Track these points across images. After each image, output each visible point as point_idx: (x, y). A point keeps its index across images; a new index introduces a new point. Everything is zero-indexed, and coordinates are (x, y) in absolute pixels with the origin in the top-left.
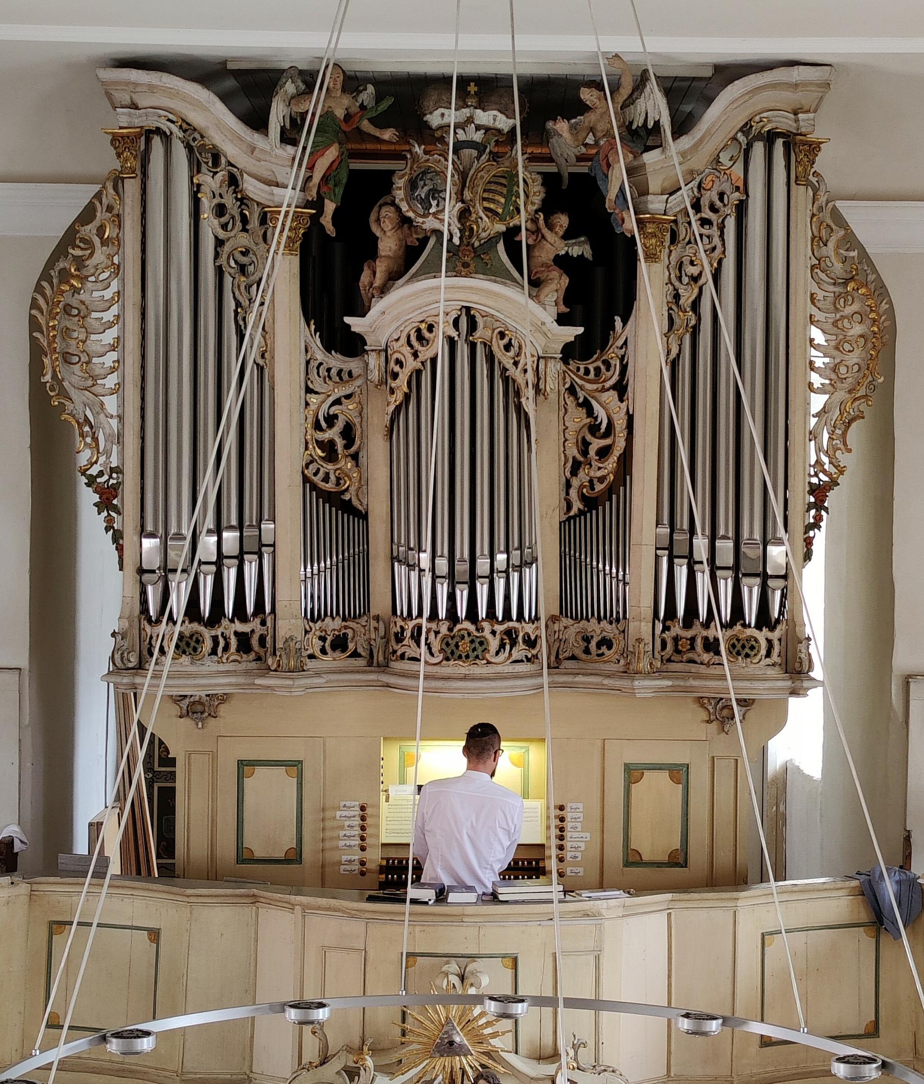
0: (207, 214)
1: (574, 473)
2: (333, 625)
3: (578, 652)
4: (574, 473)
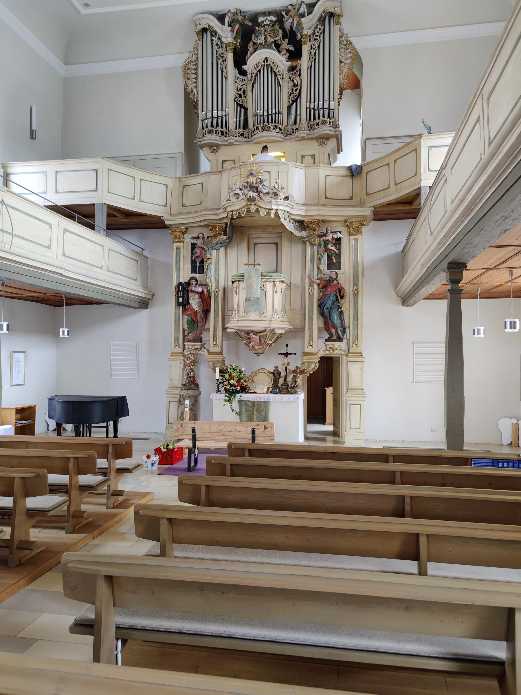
0: (215, 43)
2: (241, 131)
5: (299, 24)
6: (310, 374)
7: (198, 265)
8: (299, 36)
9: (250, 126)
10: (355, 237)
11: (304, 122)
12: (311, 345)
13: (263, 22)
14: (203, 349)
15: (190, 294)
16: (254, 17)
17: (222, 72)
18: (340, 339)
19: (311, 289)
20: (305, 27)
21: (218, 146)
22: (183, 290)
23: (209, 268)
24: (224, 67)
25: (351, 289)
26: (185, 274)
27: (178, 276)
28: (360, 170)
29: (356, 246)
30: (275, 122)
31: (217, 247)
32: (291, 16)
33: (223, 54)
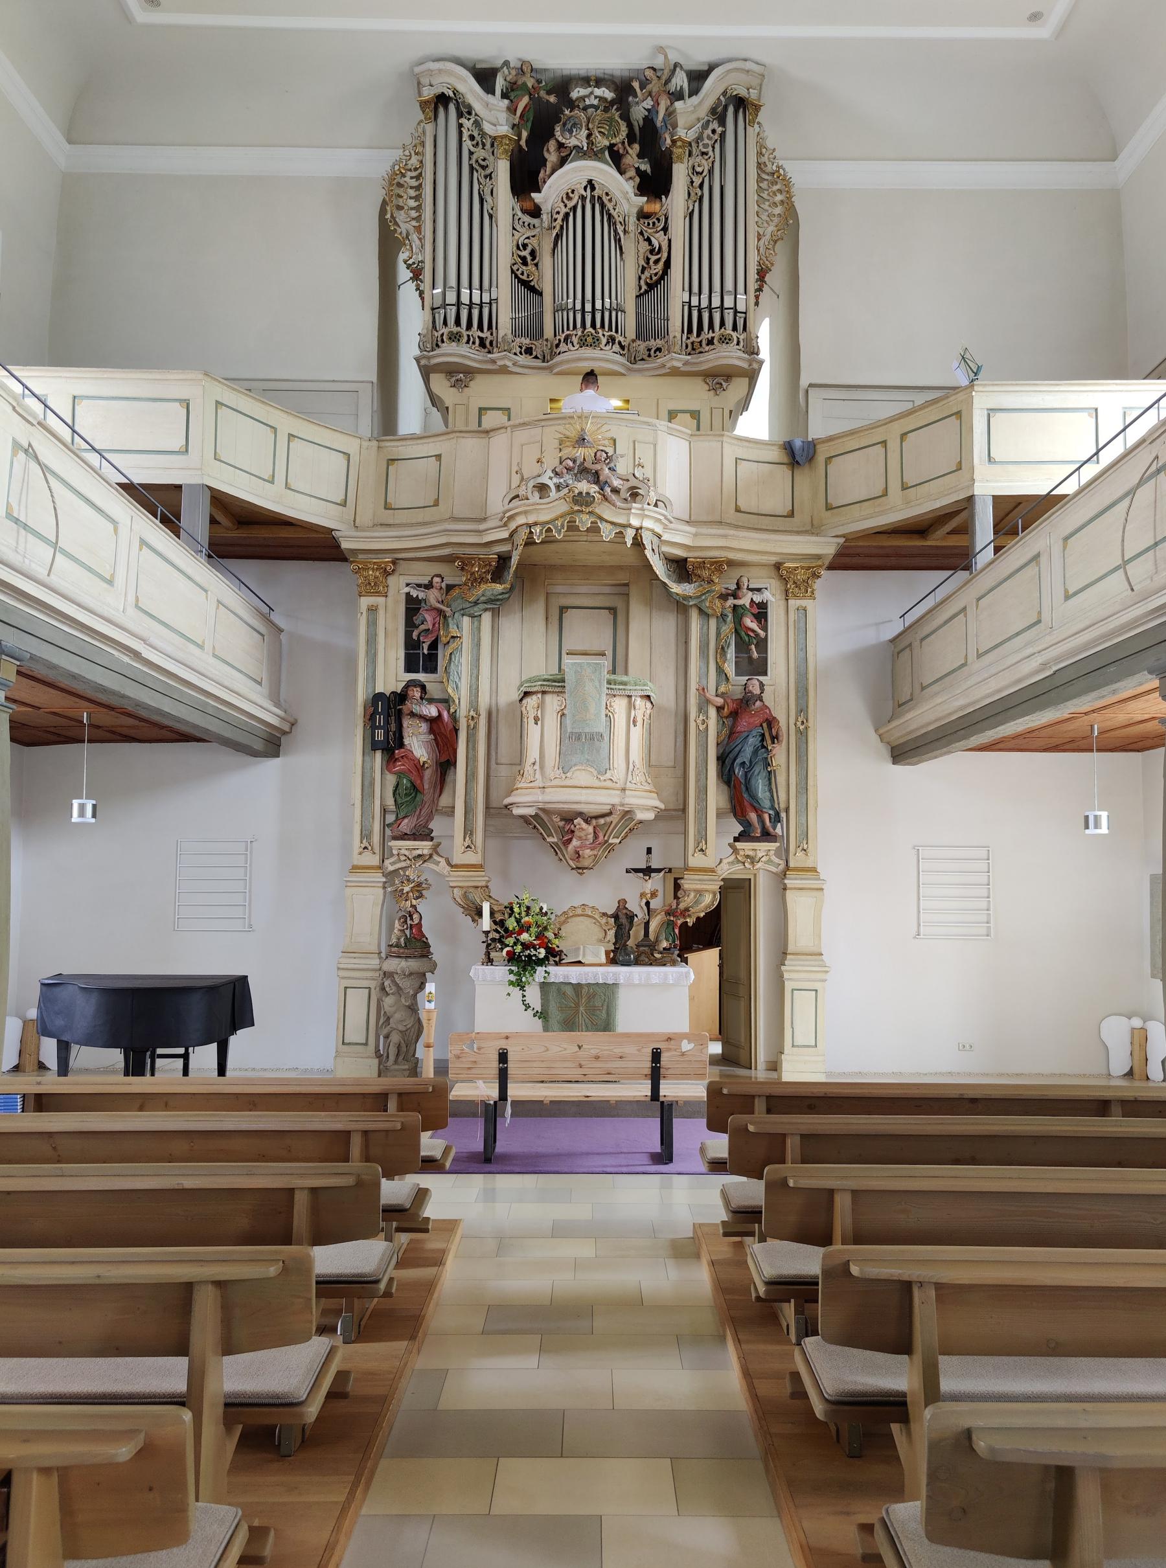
0: (465, 137)
1: (643, 272)
2: (526, 341)
3: (645, 357)
4: (643, 272)
5: (670, 113)
6: (698, 918)
7: (426, 652)
8: (668, 141)
9: (548, 331)
10: (799, 603)
11: (678, 335)
12: (702, 850)
13: (583, 98)
14: (435, 857)
15: (406, 722)
16: (562, 86)
17: (482, 201)
18: (767, 836)
19: (701, 717)
20: (681, 122)
21: (470, 372)
22: (387, 713)
23: (456, 659)
24: (487, 191)
25: (792, 721)
26: (391, 674)
27: (372, 678)
28: (811, 451)
29: (802, 625)
30: (610, 329)
31: (476, 610)
32: (650, 94)
33: (484, 160)
